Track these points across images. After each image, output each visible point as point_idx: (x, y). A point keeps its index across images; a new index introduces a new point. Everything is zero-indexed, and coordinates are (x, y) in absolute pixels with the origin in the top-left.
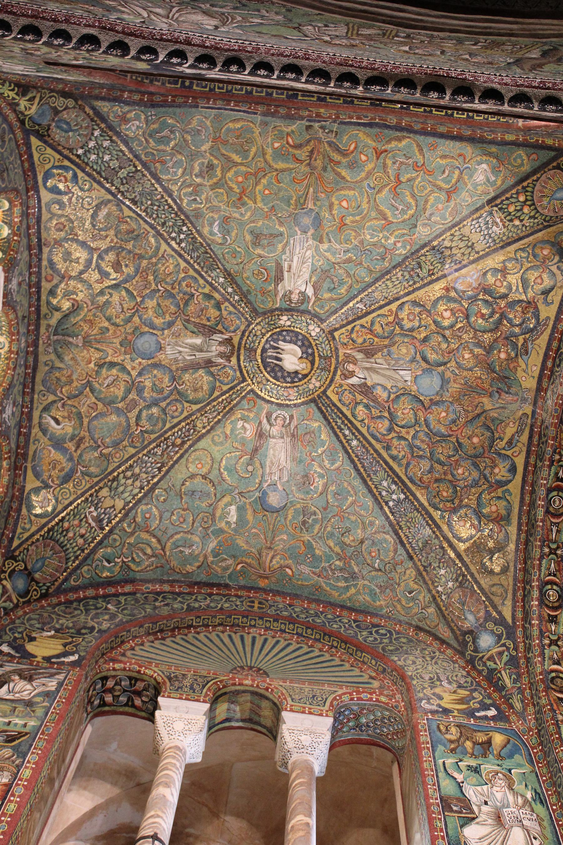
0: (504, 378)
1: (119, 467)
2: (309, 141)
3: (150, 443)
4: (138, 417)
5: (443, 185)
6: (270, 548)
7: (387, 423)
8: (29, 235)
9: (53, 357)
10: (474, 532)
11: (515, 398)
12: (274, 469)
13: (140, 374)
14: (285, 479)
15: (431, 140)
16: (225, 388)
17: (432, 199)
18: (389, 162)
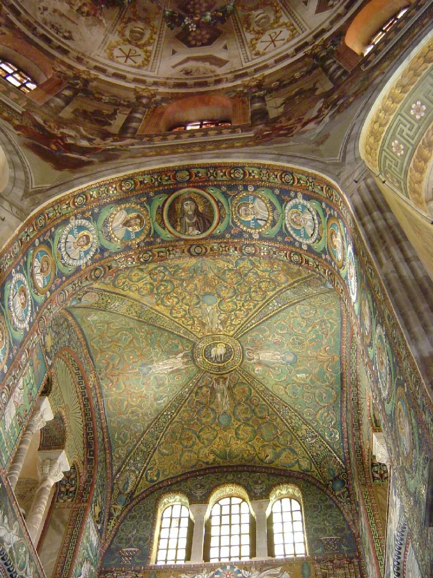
0: (195, 271)
1: (287, 426)
2: (108, 378)
3: (274, 411)
4: (261, 418)
5: (106, 326)
6: (317, 358)
7: (237, 312)
8: (181, 481)
9: (238, 458)
10: (281, 275)
11: (203, 264)
12: (275, 358)
13: (239, 420)
14: (278, 353)
15: (87, 337)
16: (241, 378)
17: (114, 328)
18: (105, 347)
